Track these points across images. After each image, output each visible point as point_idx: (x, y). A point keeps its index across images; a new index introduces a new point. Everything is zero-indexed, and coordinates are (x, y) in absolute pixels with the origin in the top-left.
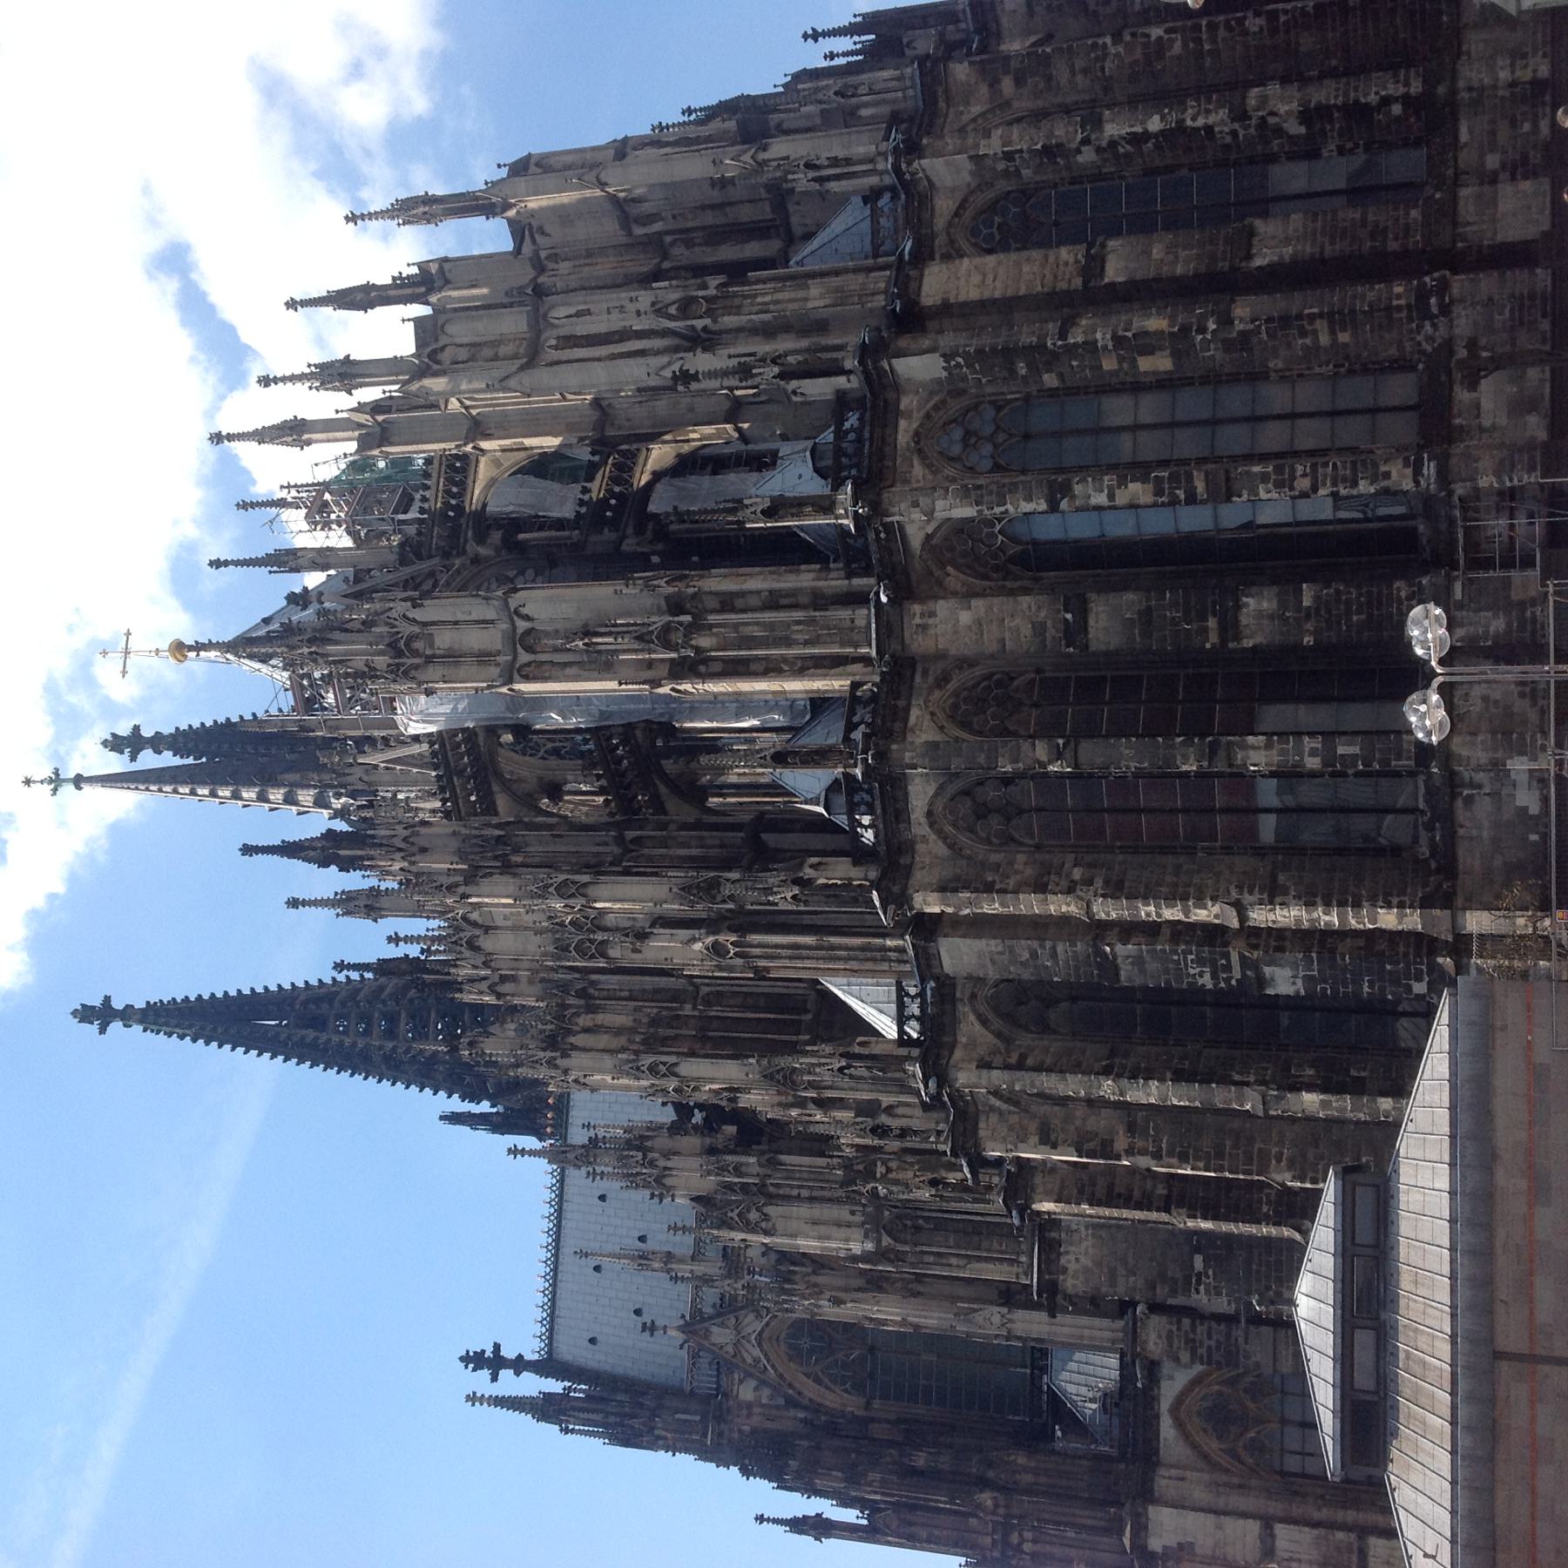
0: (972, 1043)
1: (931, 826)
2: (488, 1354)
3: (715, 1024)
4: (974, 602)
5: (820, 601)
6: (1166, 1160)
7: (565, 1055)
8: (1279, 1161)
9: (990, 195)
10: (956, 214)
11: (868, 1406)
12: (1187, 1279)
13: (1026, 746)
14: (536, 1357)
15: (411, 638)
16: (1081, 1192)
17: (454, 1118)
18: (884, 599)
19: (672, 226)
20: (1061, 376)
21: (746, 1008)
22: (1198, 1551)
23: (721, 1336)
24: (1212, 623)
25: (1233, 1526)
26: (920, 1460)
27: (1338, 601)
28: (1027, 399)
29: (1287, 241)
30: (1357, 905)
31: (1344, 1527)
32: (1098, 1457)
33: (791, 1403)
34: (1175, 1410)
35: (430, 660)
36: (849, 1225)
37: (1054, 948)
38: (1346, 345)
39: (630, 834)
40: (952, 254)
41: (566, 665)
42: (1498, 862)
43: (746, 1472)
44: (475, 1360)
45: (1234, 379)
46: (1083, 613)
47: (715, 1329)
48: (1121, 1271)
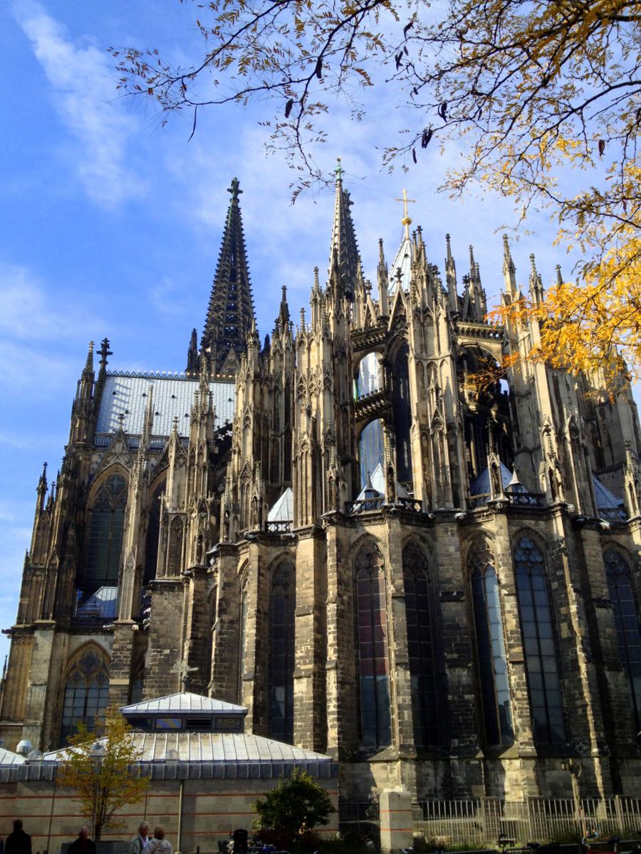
0: (268, 554)
1: (363, 535)
2: (108, 350)
3: (266, 444)
4: (458, 553)
5: (456, 487)
6: (219, 637)
7: (253, 381)
8: (220, 686)
9: (627, 558)
10: (619, 545)
11: (90, 510)
12: (159, 647)
13: (401, 575)
14: (107, 370)
15: (431, 317)
16: (198, 600)
18: (458, 515)
19: (600, 424)
20: (557, 590)
21: (272, 456)
22: (35, 652)
23: (119, 447)
24: (455, 656)
25: (45, 667)
26: (71, 532)
27: (467, 710)
28: (546, 575)
29: (617, 686)
30: (339, 719)
31: (45, 715)
32: (72, 609)
33: (91, 477)
34: (92, 642)
35: (422, 325)
37: (311, 588)
38: (576, 712)
39: (348, 408)
40: (603, 543)
41: (423, 381)
42: (359, 781)
43: (65, 459)
44: (106, 345)
45: (559, 664)
46: (457, 600)
47: (121, 445)
48: (162, 618)
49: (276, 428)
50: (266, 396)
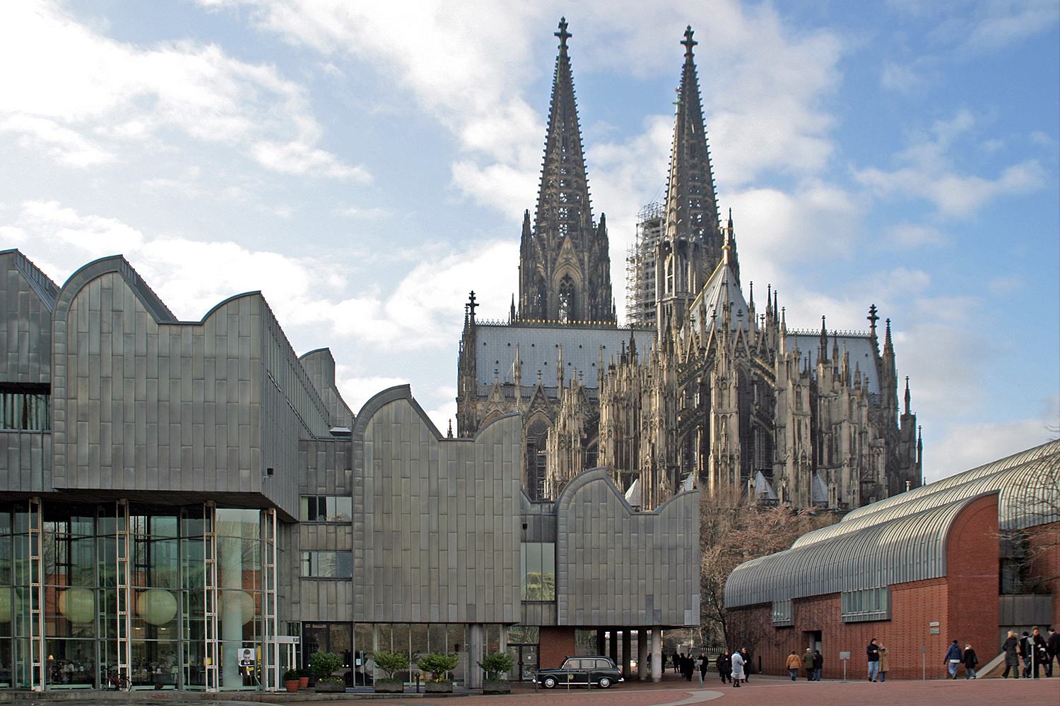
14: (476, 320)
17: (527, 216)
35: (721, 389)
36: (562, 472)
39: (674, 432)
49: (628, 433)
50: (621, 411)
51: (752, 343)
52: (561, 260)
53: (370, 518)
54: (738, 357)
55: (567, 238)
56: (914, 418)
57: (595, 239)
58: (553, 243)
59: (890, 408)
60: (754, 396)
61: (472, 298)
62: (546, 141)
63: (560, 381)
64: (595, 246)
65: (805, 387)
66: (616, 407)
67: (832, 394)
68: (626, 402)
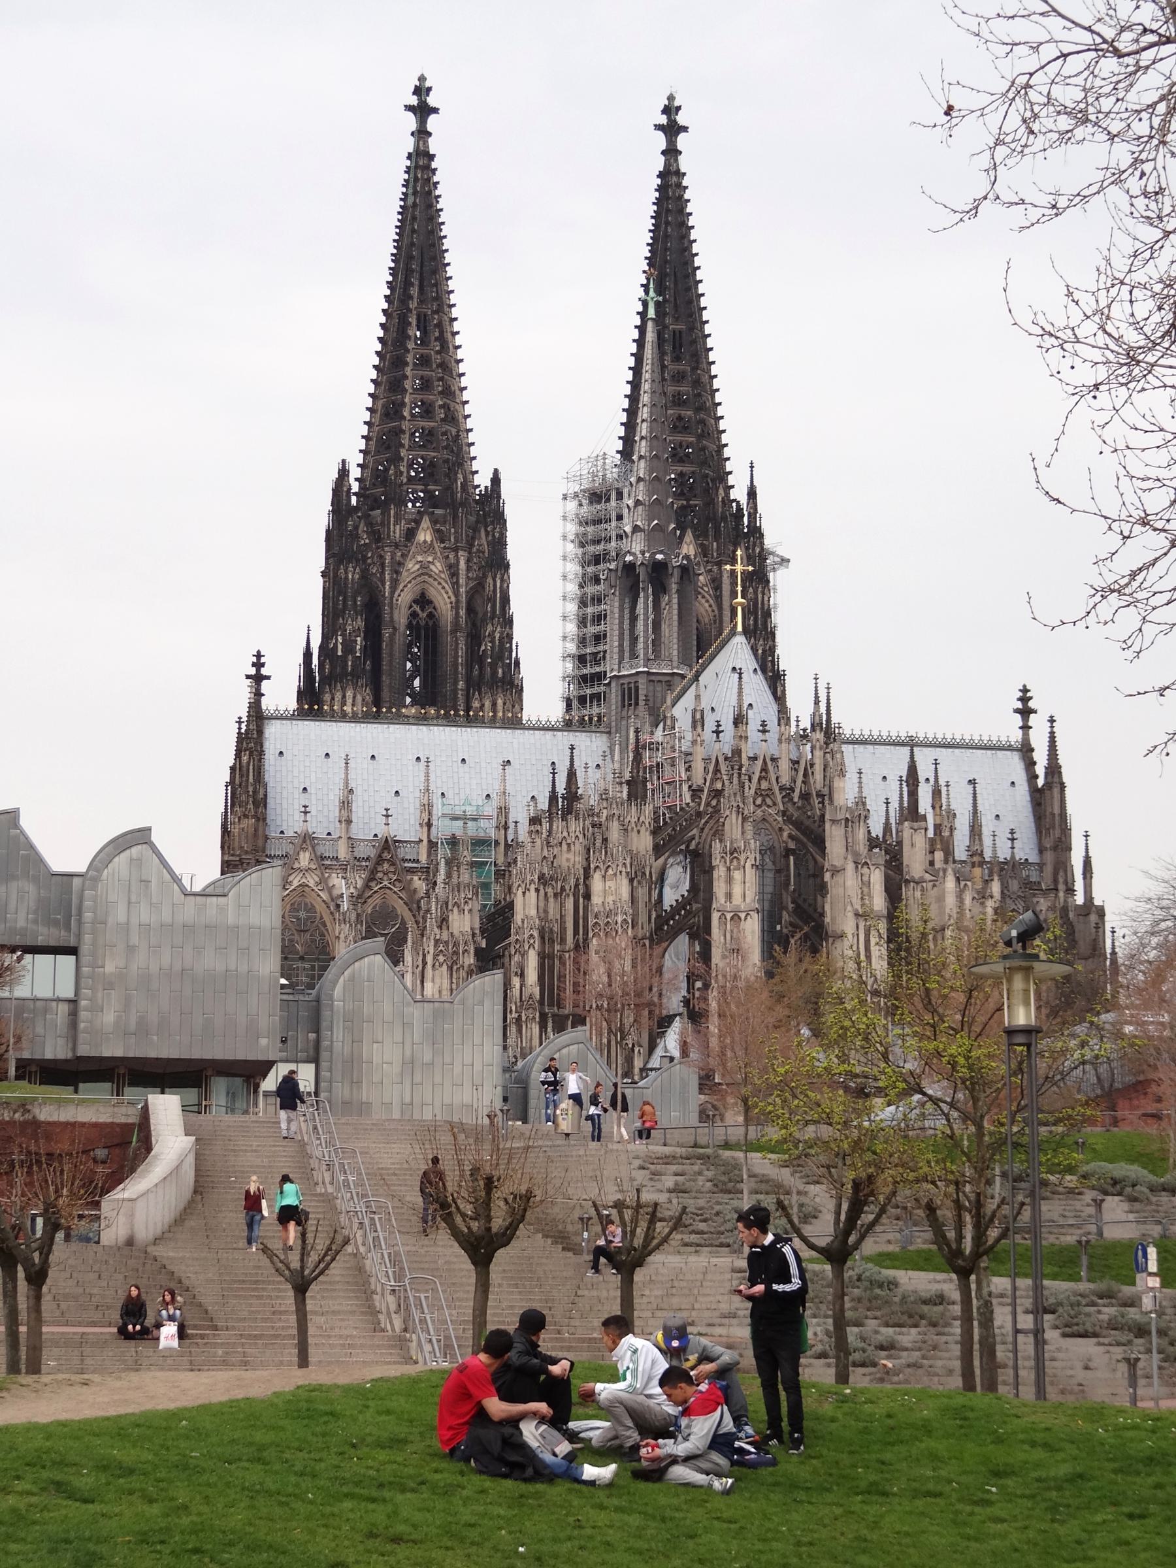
14: (264, 707)
17: (343, 473)
23: (304, 859)
35: (729, 869)
49: (563, 940)
50: (551, 900)
51: (785, 780)
52: (412, 566)
53: (337, 1086)
54: (760, 806)
55: (426, 523)
56: (1101, 912)
57: (479, 521)
58: (397, 532)
59: (1057, 890)
60: (788, 876)
61: (258, 665)
62: (383, 320)
63: (425, 829)
64: (480, 538)
65: (877, 866)
66: (542, 892)
67: (928, 877)
68: (559, 884)
